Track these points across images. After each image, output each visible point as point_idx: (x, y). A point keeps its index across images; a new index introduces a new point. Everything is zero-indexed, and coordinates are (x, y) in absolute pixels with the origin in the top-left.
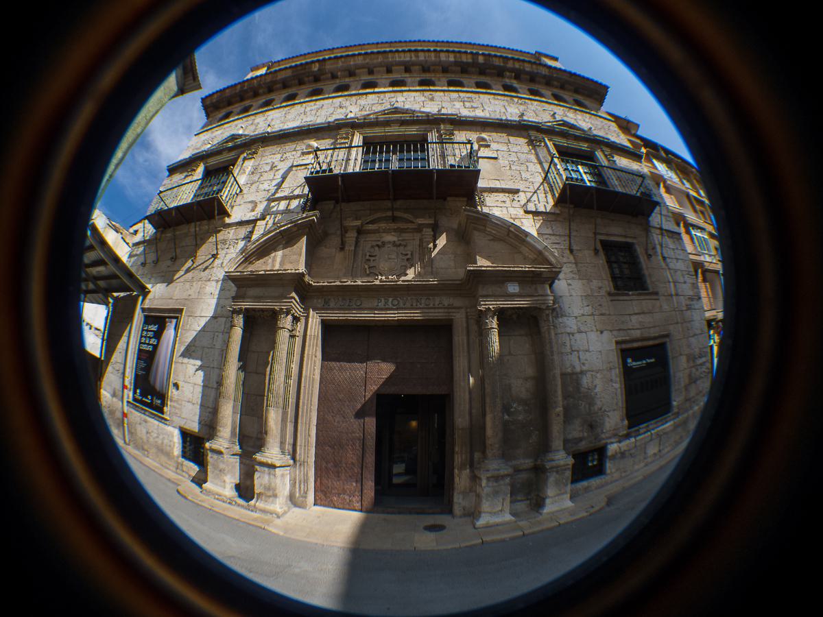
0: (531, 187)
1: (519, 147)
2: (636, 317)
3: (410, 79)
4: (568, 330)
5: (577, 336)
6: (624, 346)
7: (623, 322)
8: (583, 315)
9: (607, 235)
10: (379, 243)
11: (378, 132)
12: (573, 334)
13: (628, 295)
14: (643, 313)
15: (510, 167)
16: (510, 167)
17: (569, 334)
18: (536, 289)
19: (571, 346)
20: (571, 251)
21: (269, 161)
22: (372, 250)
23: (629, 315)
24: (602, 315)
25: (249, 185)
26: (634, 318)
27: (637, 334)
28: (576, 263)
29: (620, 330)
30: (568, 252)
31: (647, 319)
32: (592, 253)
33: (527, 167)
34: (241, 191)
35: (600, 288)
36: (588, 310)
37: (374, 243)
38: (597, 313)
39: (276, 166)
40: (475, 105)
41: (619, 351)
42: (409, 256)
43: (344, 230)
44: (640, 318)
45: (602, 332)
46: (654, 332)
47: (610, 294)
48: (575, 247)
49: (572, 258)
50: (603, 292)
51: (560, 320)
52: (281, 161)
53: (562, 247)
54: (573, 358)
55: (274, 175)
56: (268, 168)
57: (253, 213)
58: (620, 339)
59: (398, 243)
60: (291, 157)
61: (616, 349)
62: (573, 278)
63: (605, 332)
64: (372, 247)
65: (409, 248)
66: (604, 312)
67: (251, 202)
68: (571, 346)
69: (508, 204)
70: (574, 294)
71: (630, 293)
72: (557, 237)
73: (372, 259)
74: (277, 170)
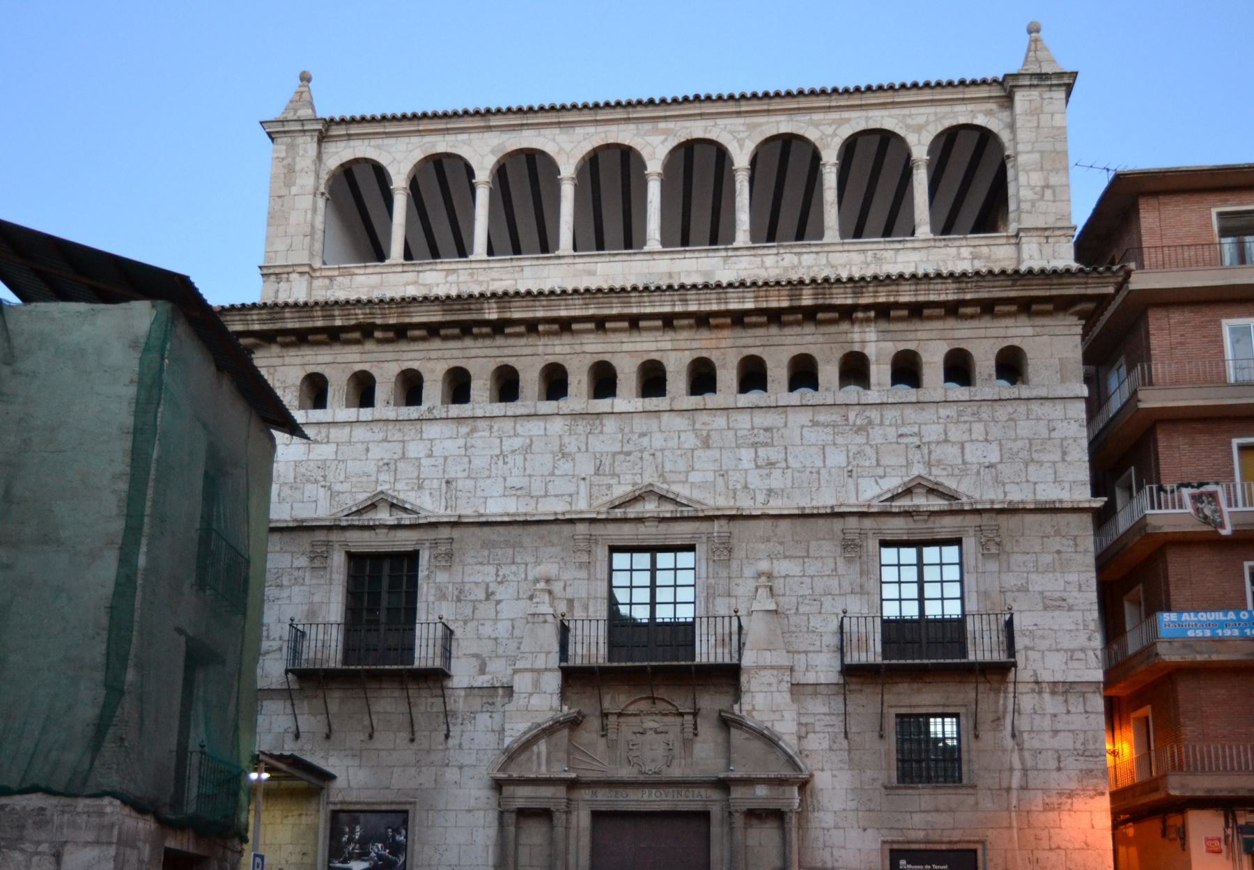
0: (818, 643)
1: (820, 564)
2: (923, 815)
3: (672, 355)
4: (823, 825)
5: (833, 832)
6: (895, 846)
7: (899, 820)
8: (844, 810)
9: (910, 706)
10: (641, 730)
11: (627, 534)
12: (828, 830)
13: (918, 788)
14: (937, 810)
15: (797, 609)
16: (797, 609)
17: (824, 829)
18: (784, 791)
19: (824, 842)
20: (846, 736)
21: (479, 578)
22: (634, 737)
23: (911, 812)
24: (870, 810)
25: (461, 623)
26: (917, 818)
27: (921, 835)
28: (849, 751)
29: (892, 828)
30: (843, 735)
31: (943, 820)
32: (876, 735)
33: (821, 604)
34: (452, 632)
35: (874, 780)
36: (853, 805)
37: (636, 730)
38: (863, 808)
39: (493, 593)
40: (774, 454)
41: (887, 853)
42: (671, 747)
43: (605, 715)
44: (929, 817)
45: (865, 830)
46: (956, 835)
47: (886, 788)
48: (853, 729)
49: (845, 743)
50: (878, 785)
51: (816, 814)
52: (501, 583)
53: (837, 730)
54: (826, 855)
55: (497, 612)
56: (482, 596)
57: (486, 678)
58: (889, 839)
59: (659, 730)
60: (512, 577)
61: (882, 849)
62: (841, 769)
63: (869, 832)
64: (635, 733)
65: (670, 737)
66: (872, 807)
67: (476, 656)
68: (824, 842)
69: (774, 688)
70: (838, 787)
71: (920, 785)
72: (833, 717)
73: (635, 747)
74: (498, 602)
